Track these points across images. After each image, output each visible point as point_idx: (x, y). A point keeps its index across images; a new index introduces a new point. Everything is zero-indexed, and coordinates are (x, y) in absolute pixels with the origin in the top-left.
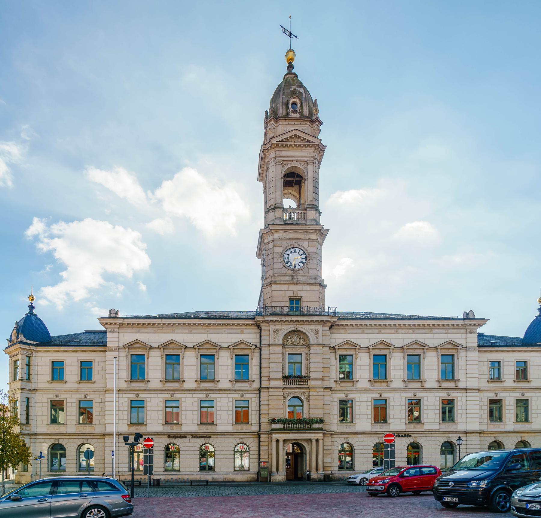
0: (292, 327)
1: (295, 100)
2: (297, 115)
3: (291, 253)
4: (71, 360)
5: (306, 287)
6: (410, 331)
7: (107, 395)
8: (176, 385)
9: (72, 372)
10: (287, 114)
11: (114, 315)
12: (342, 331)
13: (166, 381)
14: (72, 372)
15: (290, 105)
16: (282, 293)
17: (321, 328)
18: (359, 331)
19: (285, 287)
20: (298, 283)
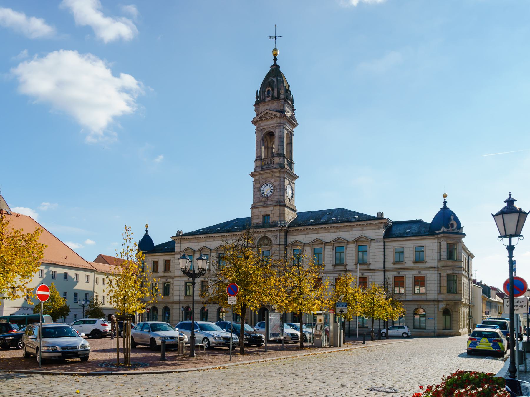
0: (262, 235)
2: (270, 98)
4: (161, 259)
5: (272, 208)
6: (338, 231)
7: (175, 279)
8: (365, 267)
9: (161, 267)
10: (265, 99)
11: (179, 233)
12: (295, 234)
13: (336, 265)
14: (161, 267)
15: (266, 93)
16: (258, 213)
17: (278, 234)
18: (306, 233)
19: (260, 210)
20: (267, 207)
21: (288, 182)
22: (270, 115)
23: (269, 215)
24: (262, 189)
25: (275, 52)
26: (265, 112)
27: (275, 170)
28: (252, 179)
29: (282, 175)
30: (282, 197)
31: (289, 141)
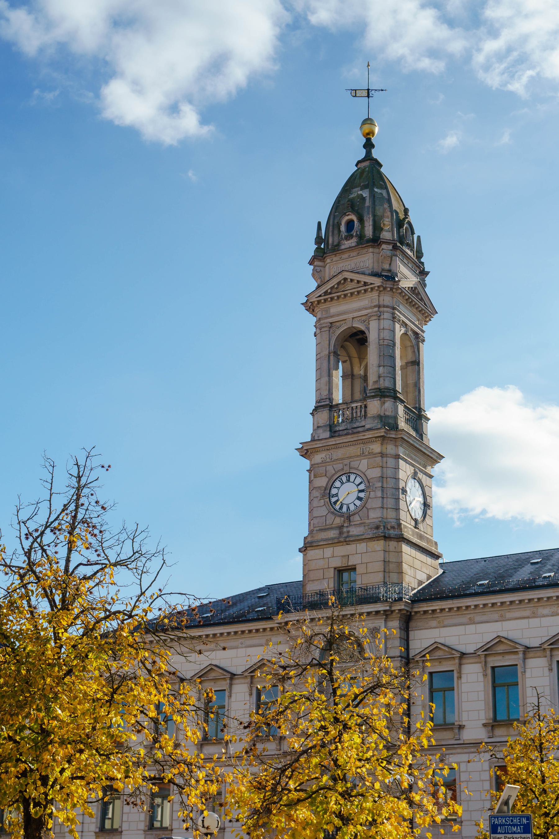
1: (346, 218)
3: (342, 483)
5: (362, 547)
10: (339, 245)
12: (434, 623)
16: (322, 564)
17: (380, 622)
18: (464, 619)
19: (328, 552)
20: (347, 542)
21: (410, 470)
22: (354, 285)
23: (353, 569)
24: (334, 491)
25: (367, 128)
26: (340, 278)
27: (369, 435)
28: (306, 464)
29: (390, 449)
30: (391, 514)
31: (410, 357)
